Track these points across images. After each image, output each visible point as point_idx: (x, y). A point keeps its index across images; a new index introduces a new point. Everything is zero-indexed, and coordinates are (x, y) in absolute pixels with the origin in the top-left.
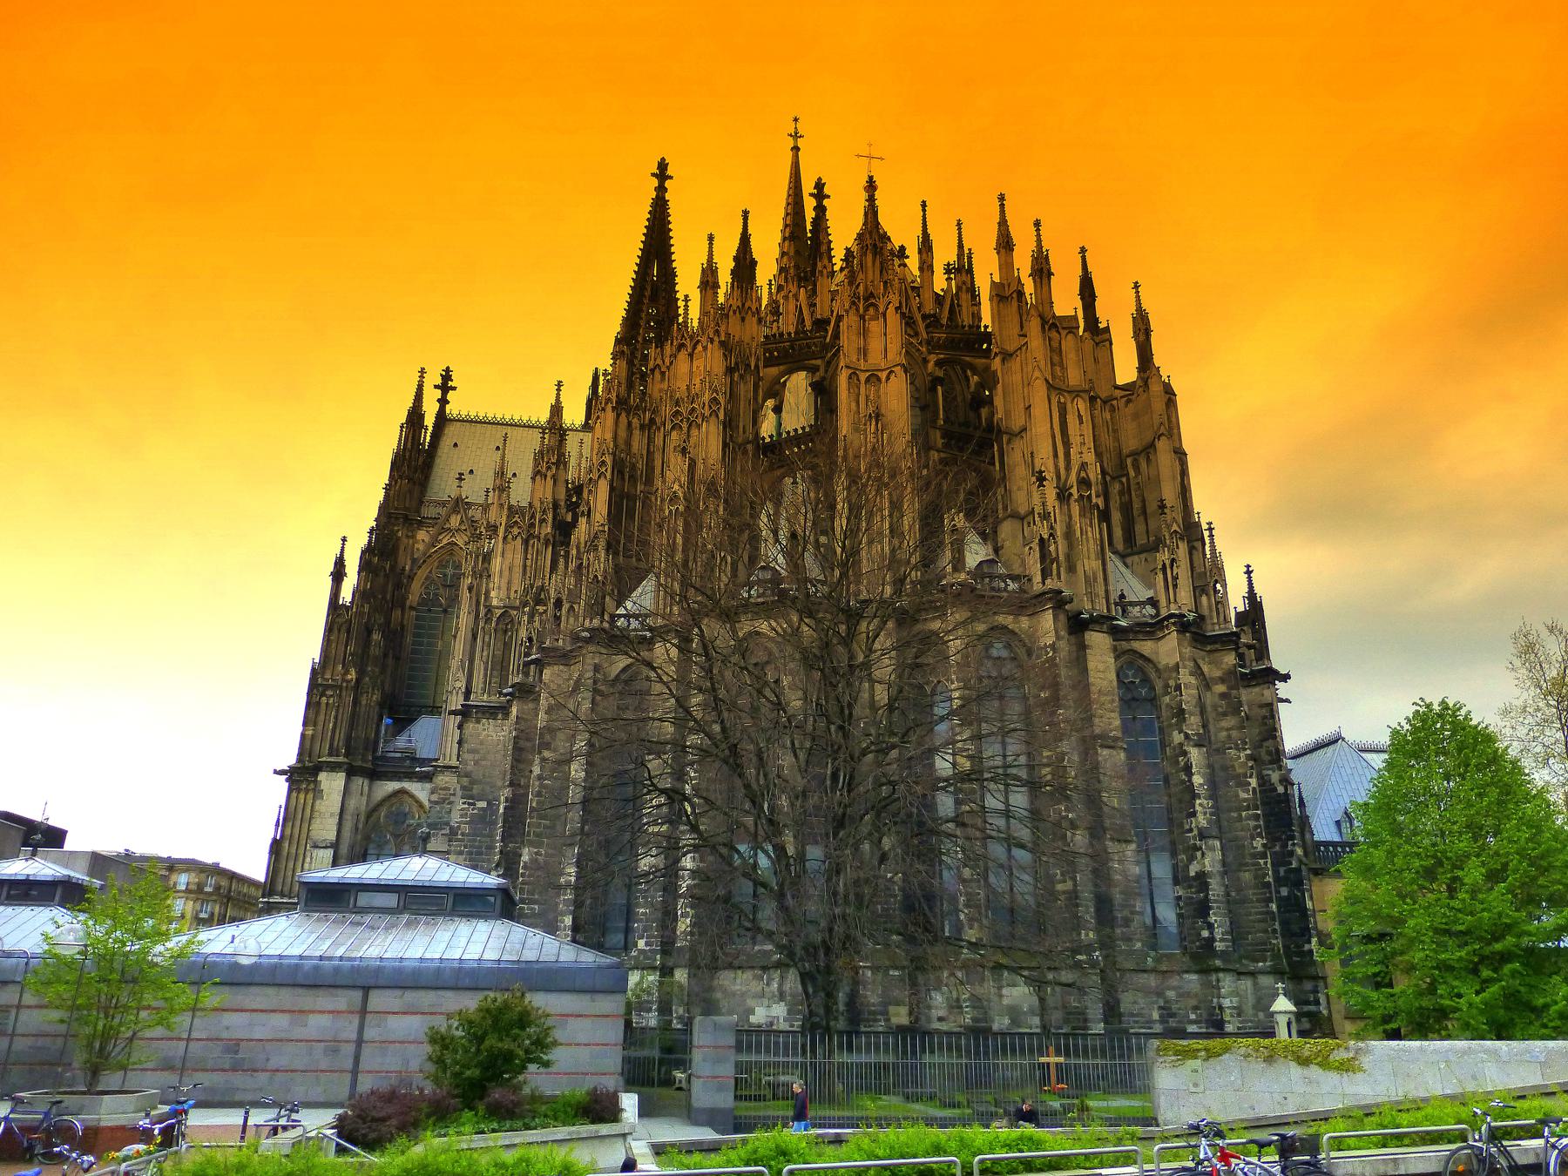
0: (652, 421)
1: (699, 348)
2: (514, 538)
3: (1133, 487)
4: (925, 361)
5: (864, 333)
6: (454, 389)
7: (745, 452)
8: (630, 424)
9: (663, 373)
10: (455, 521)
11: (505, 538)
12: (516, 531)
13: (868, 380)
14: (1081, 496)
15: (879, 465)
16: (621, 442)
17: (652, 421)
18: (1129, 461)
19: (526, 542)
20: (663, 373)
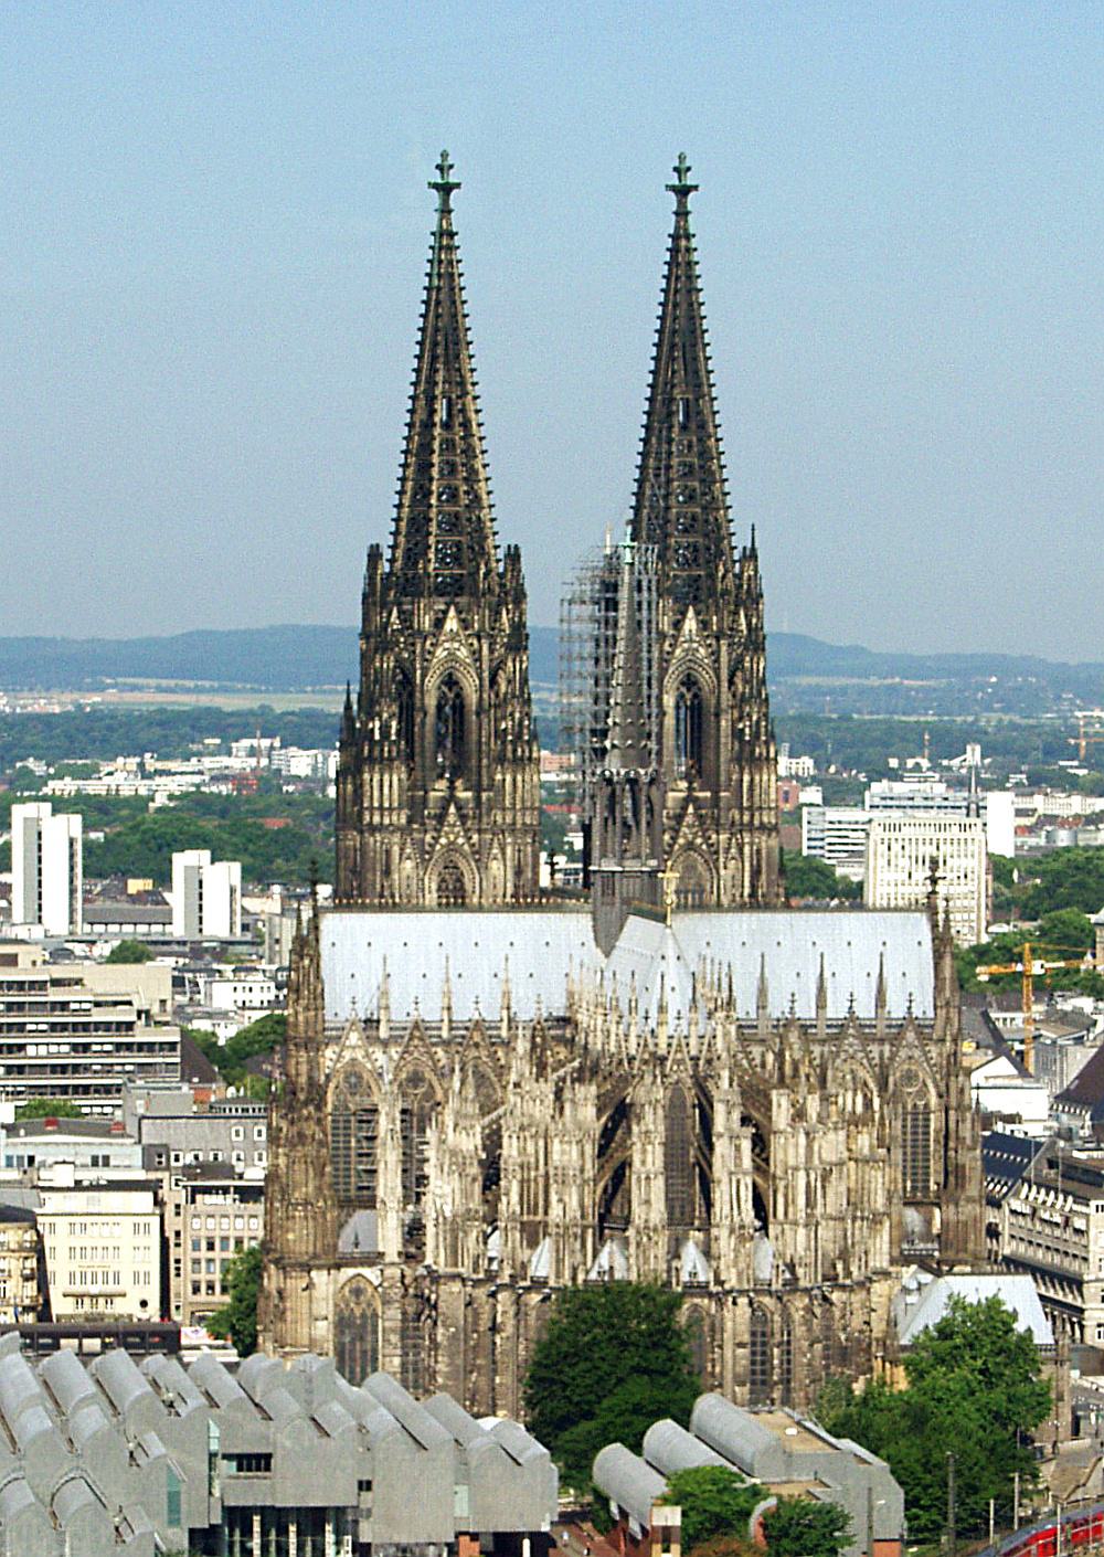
5: (644, 1151)
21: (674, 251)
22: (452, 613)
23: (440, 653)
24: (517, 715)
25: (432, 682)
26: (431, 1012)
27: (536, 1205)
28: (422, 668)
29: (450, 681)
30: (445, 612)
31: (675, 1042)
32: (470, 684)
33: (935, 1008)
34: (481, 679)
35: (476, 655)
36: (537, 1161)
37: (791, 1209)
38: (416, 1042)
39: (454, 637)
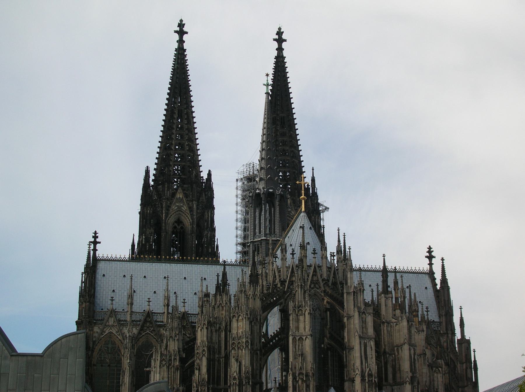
0: (220, 328)
1: (240, 318)
2: (163, 366)
3: (397, 359)
4: (323, 299)
5: (298, 321)
6: (100, 243)
7: (257, 354)
8: (211, 330)
9: (223, 307)
10: (111, 321)
11: (160, 366)
12: (164, 363)
13: (299, 339)
14: (369, 381)
15: (303, 374)
16: (209, 338)
17: (220, 328)
18: (396, 348)
19: (168, 367)
20: (223, 307)
21: (276, 63)
22: (180, 190)
23: (174, 207)
24: (209, 235)
25: (171, 220)
26: (158, 307)
27: (219, 377)
28: (165, 213)
29: (179, 221)
30: (177, 189)
31: (312, 268)
32: (187, 221)
33: (440, 317)
34: (192, 219)
35: (191, 209)
36: (220, 347)
37: (398, 375)
38: (148, 324)
39: (181, 200)
